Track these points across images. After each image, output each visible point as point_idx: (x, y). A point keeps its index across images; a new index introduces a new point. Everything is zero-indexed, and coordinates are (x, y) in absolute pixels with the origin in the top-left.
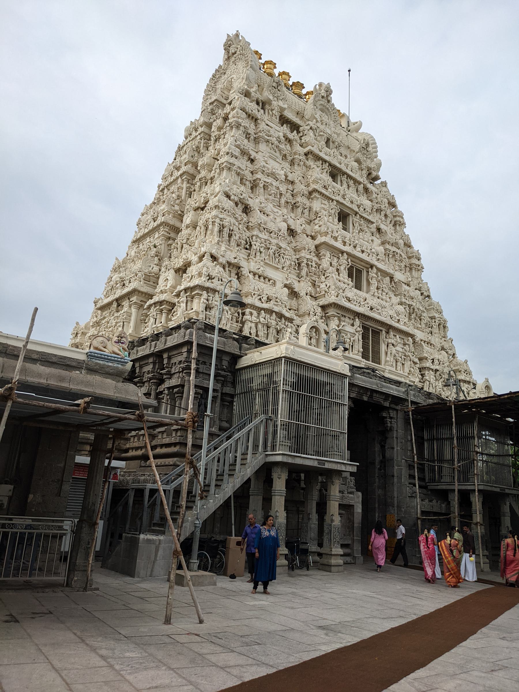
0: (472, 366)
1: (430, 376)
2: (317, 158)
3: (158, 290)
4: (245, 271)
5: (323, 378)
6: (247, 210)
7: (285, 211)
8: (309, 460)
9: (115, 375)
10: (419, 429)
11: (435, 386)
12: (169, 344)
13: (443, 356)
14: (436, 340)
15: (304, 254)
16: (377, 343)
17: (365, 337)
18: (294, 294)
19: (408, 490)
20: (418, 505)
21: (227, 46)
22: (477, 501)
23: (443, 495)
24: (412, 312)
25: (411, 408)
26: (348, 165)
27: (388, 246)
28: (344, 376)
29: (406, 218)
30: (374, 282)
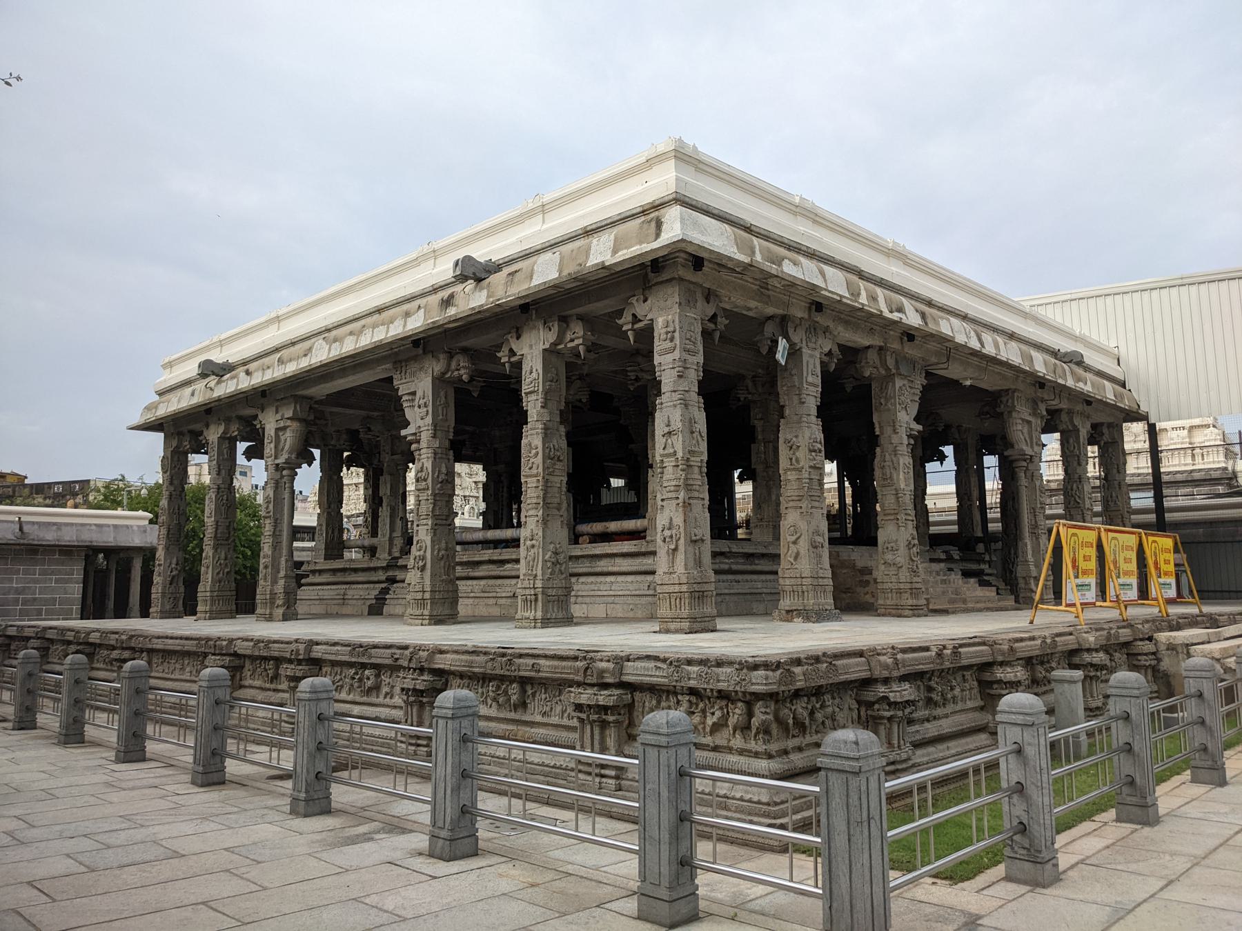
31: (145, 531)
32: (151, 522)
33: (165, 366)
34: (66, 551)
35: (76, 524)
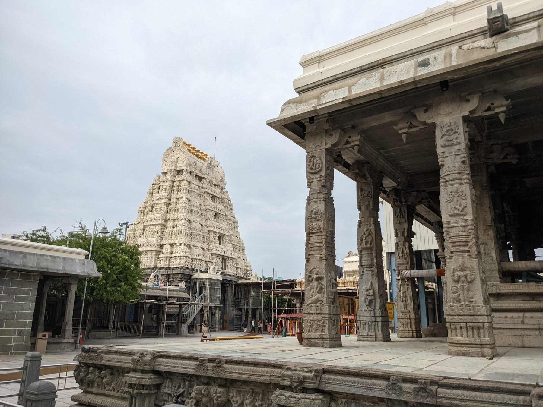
0: (251, 264)
1: (239, 270)
2: (208, 193)
3: (164, 251)
4: (192, 246)
5: (216, 282)
6: (190, 222)
7: (200, 219)
8: (213, 305)
9: (182, 291)
10: (235, 288)
11: (241, 274)
12: (174, 273)
13: (243, 262)
14: (241, 255)
15: (205, 234)
16: (225, 263)
17: (222, 262)
18: (203, 249)
19: (231, 309)
20: (234, 313)
21: (175, 142)
22: (250, 311)
23: (240, 309)
24: (235, 247)
25: (234, 283)
26: (216, 191)
27: (228, 221)
28: (219, 280)
29: (234, 207)
30: (224, 240)
31: (84, 264)
32: (87, 257)
33: (305, 64)
34: (26, 274)
35: (37, 255)
